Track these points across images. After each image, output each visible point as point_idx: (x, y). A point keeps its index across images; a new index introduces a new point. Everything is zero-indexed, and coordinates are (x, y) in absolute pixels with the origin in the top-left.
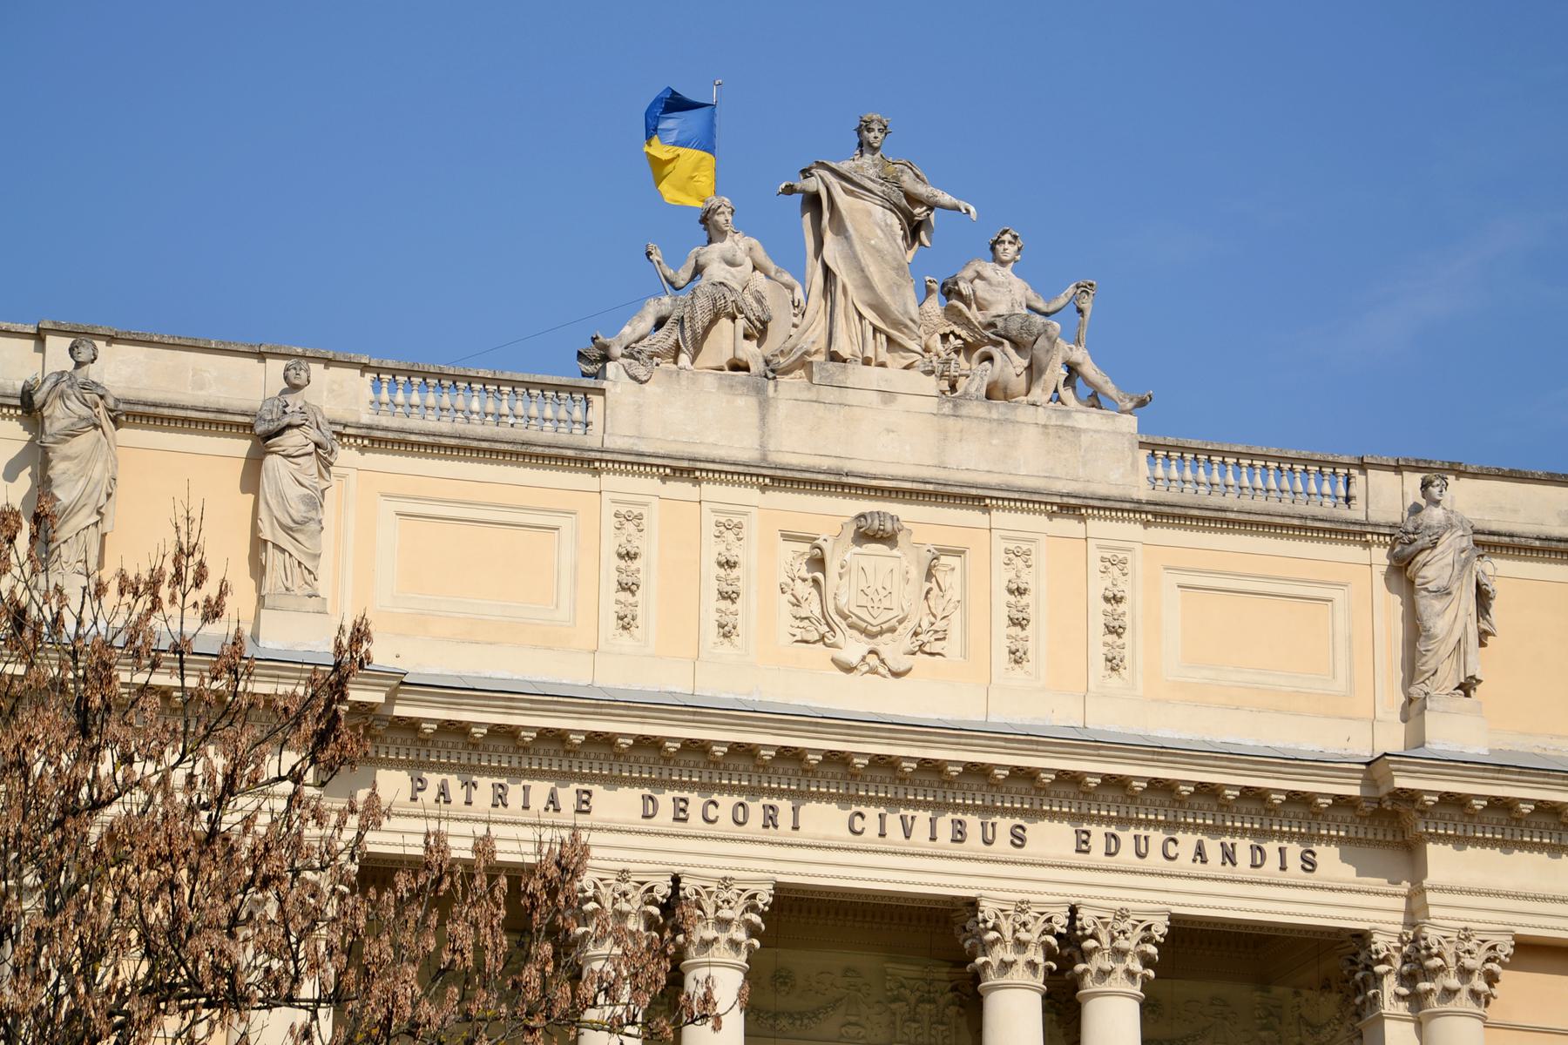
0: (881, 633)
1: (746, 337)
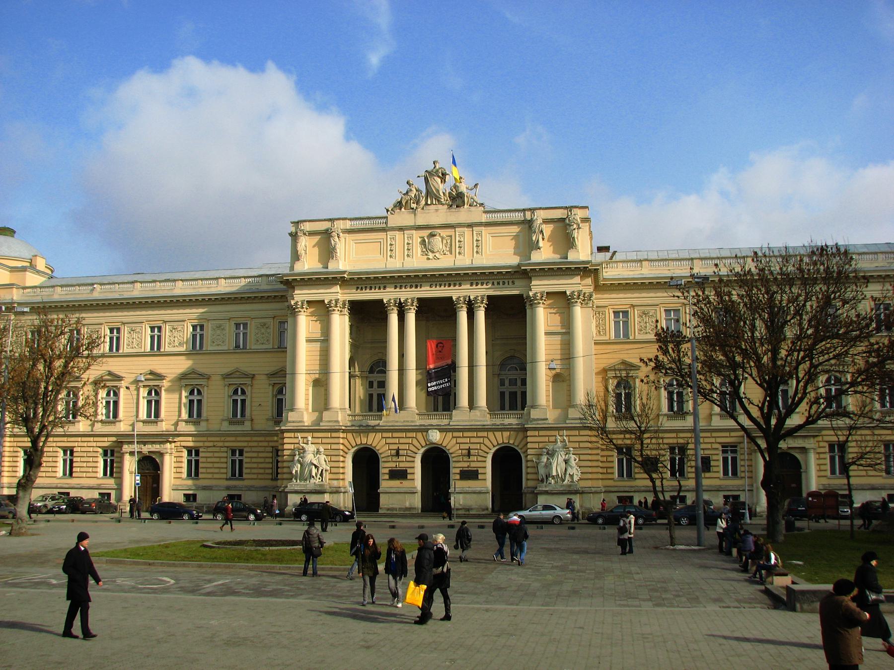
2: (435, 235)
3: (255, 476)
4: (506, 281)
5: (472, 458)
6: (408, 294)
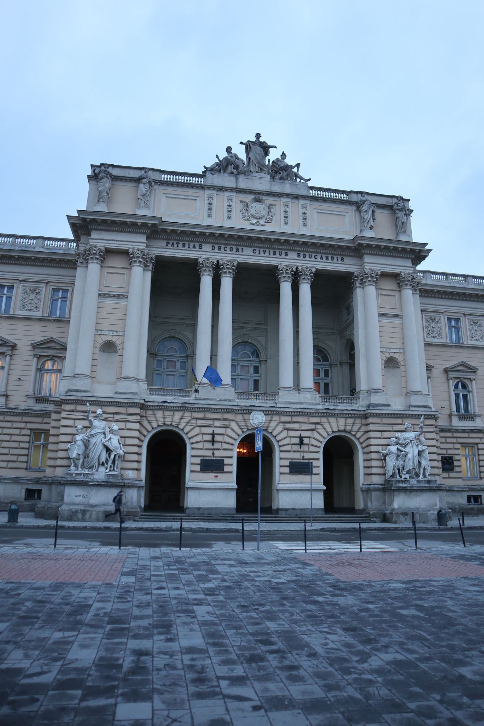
0: (259, 219)
1: (234, 169)
4: (335, 257)
6: (230, 257)
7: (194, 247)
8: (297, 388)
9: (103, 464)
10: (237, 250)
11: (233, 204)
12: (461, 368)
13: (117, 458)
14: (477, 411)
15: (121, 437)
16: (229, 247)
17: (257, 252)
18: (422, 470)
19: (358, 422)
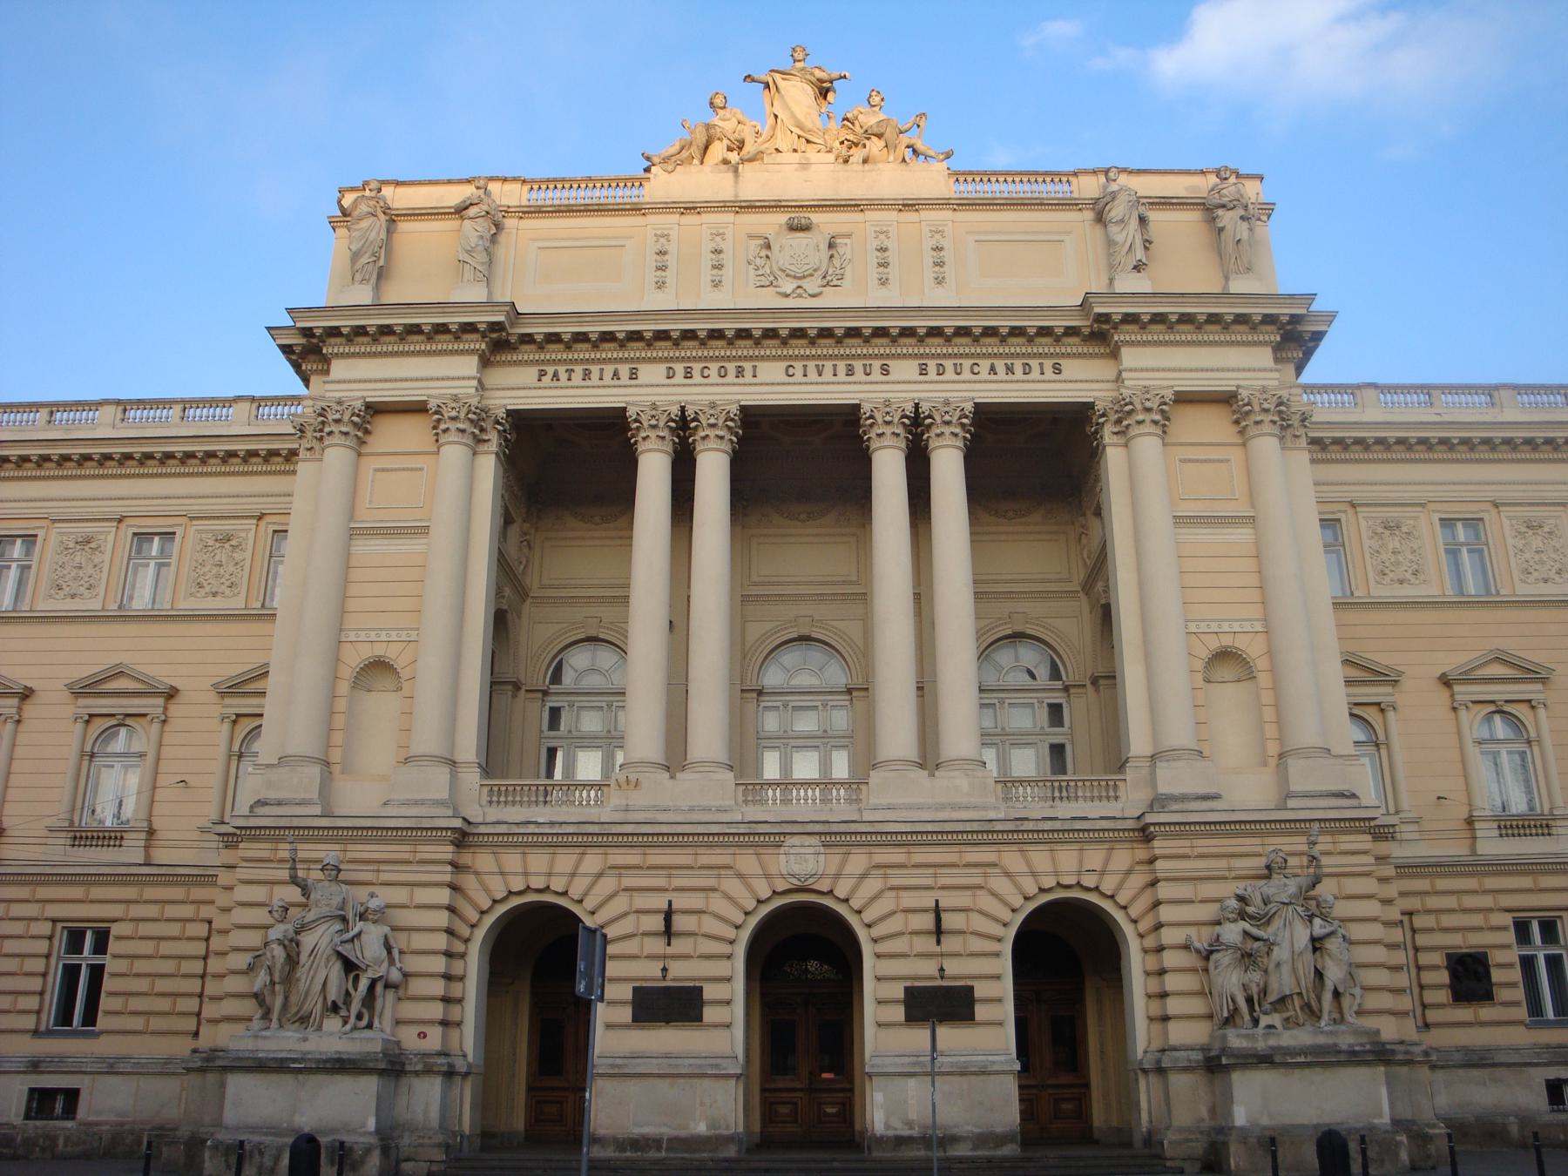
1: (730, 149)
2: (805, 228)
3: (137, 1023)
5: (949, 944)
7: (616, 375)
8: (929, 757)
9: (335, 1008)
10: (740, 372)
11: (727, 246)
12: (1498, 670)
13: (379, 988)
14: (1559, 802)
15: (393, 929)
16: (714, 367)
17: (799, 371)
18: (1328, 997)
19: (1122, 858)
